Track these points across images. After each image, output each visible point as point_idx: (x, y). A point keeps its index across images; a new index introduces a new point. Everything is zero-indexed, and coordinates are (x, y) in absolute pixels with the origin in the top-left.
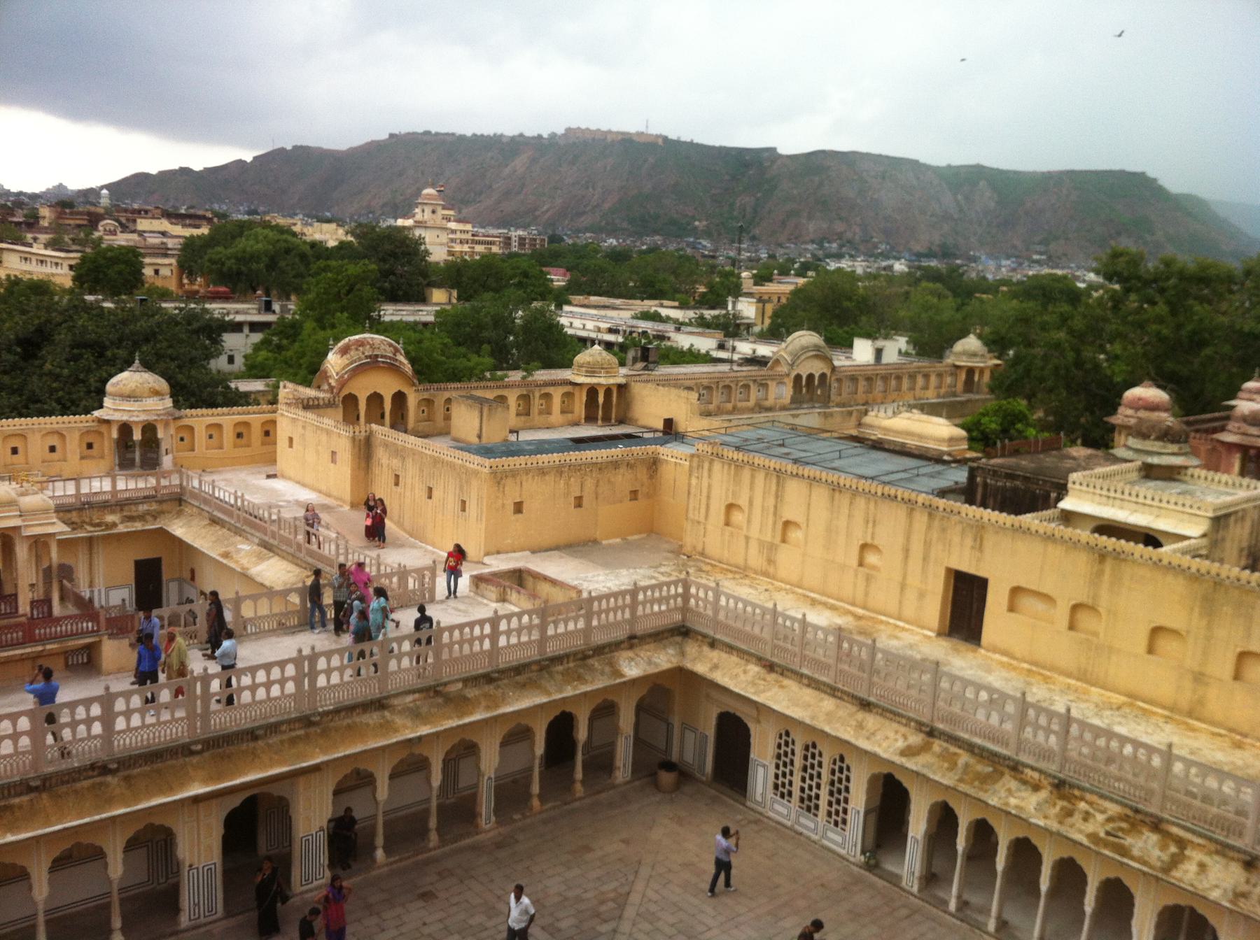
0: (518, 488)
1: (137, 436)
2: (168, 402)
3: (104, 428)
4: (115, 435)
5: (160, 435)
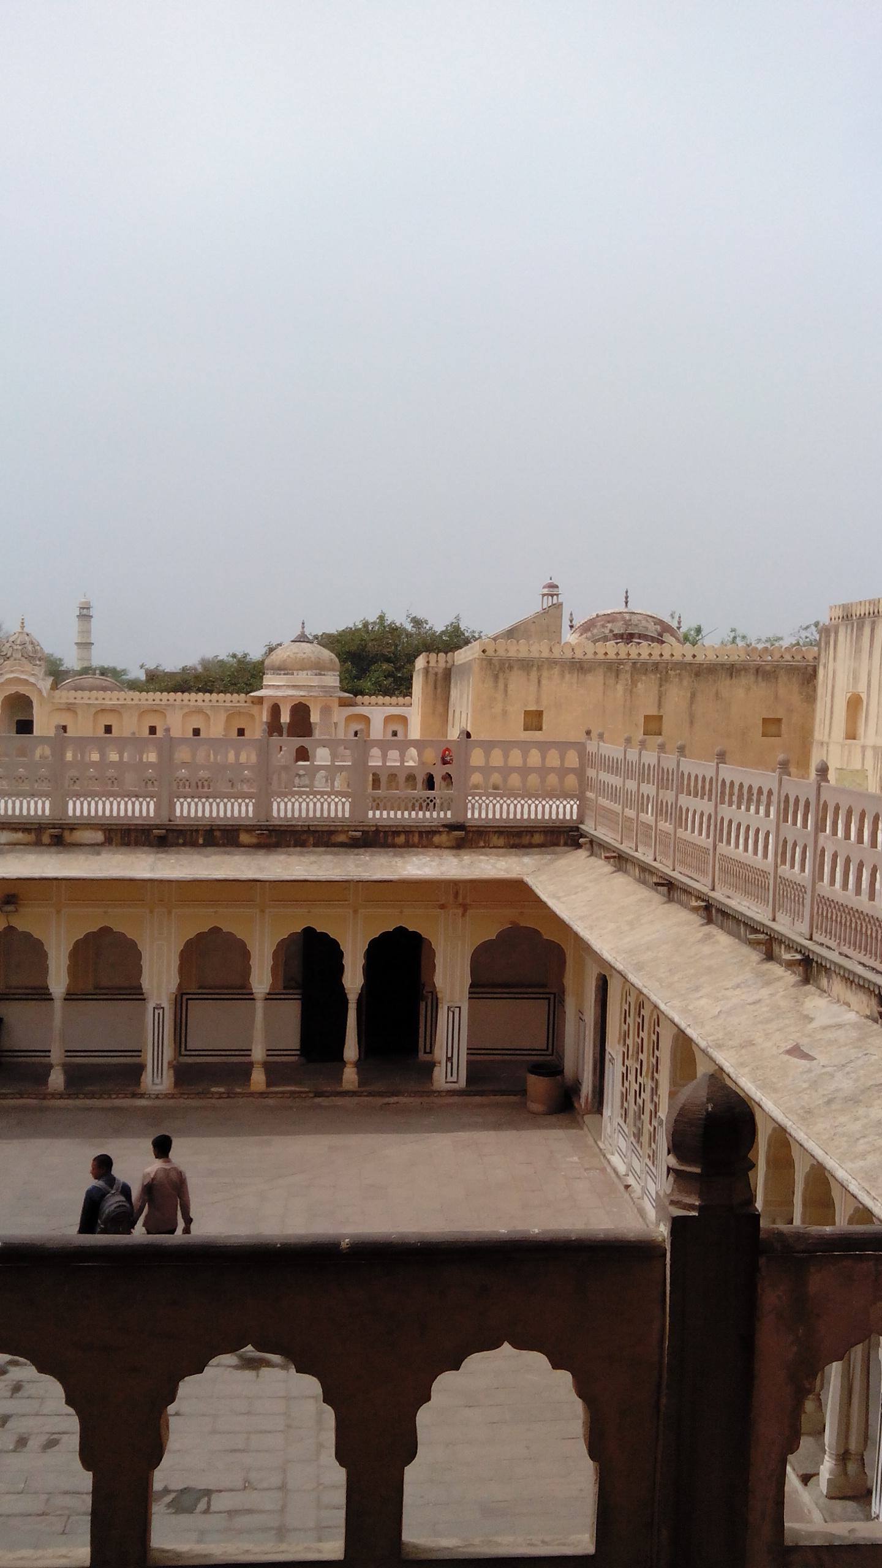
0: (533, 688)
1: (285, 718)
2: (332, 680)
3: (255, 710)
4: (265, 717)
5: (315, 718)
